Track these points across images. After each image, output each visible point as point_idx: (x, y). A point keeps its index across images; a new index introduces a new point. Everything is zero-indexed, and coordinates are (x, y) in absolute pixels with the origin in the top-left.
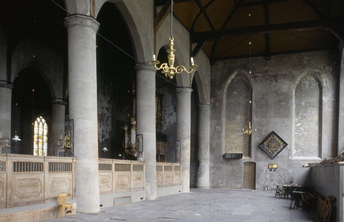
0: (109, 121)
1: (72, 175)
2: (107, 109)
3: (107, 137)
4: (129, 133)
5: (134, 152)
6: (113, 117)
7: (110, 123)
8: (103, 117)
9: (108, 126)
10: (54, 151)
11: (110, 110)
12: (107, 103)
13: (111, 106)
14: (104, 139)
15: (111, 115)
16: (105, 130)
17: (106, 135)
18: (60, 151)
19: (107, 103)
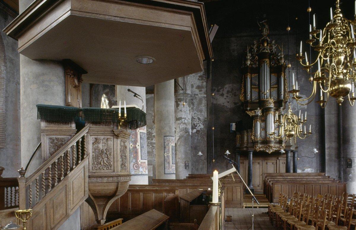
0: (203, 105)
1: (331, 189)
2: (198, 87)
3: (200, 127)
4: (264, 120)
5: (272, 147)
6: (208, 99)
7: (204, 108)
8: (192, 100)
9: (201, 111)
10: (164, 145)
11: (204, 90)
12: (198, 79)
13: (205, 84)
14: (195, 131)
15: (205, 96)
16: (196, 118)
17: (198, 125)
18: (172, 145)
19: (198, 79)
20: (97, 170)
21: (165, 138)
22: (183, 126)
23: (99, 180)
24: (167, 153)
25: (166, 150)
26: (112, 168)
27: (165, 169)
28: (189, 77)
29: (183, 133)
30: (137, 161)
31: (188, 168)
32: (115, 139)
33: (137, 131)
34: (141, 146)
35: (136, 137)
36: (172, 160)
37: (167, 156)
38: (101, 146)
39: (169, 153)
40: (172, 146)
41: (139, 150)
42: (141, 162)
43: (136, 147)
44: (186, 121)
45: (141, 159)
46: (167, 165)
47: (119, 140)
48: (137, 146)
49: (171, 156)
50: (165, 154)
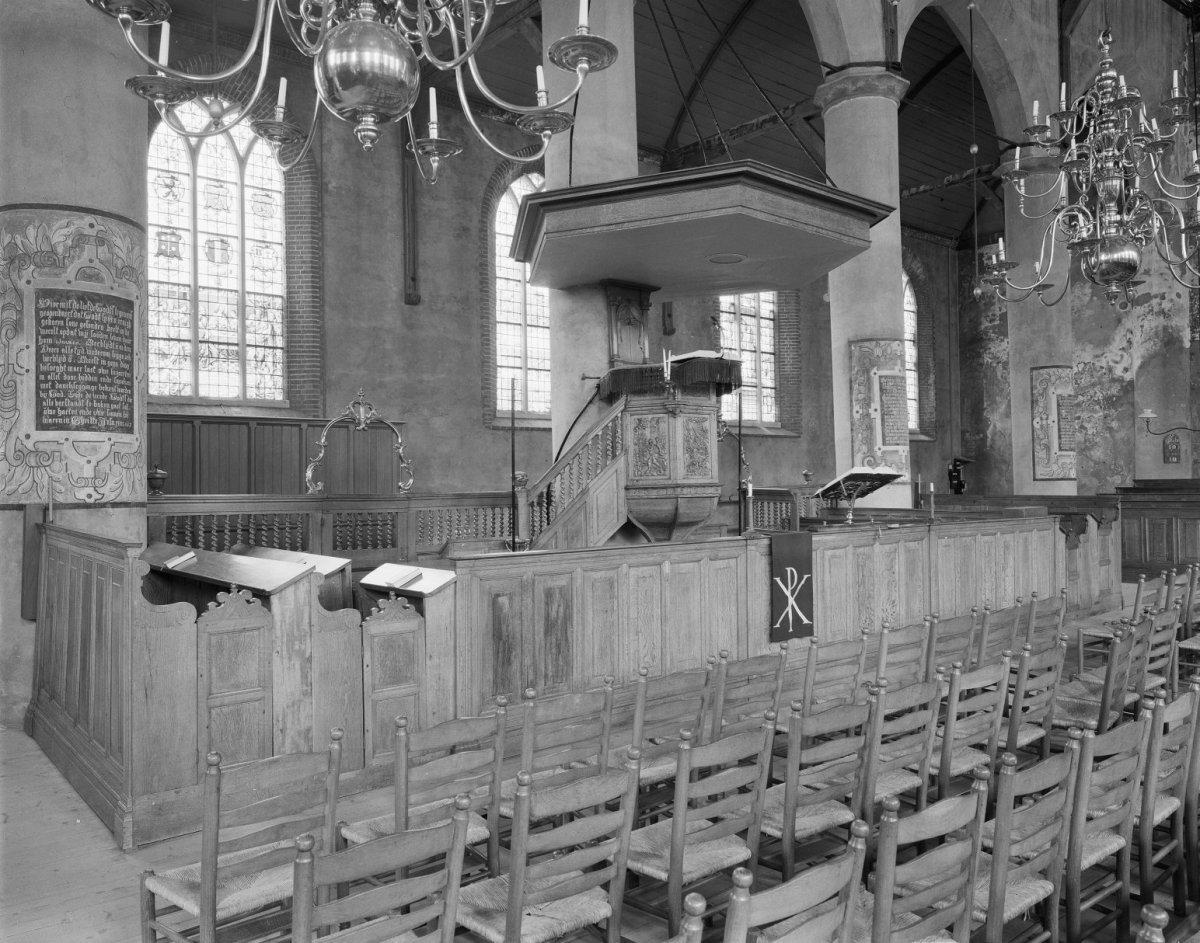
18: (1059, 392)
20: (641, 476)
21: (1035, 372)
22: (1153, 324)
23: (643, 493)
24: (1041, 419)
25: (1039, 409)
26: (667, 472)
27: (1034, 465)
28: (1172, 158)
29: (1155, 344)
30: (871, 449)
31: (1175, 459)
32: (671, 420)
33: (872, 373)
34: (882, 410)
35: (869, 389)
36: (1060, 437)
37: (1042, 426)
38: (647, 433)
39: (1047, 419)
40: (1060, 397)
41: (878, 422)
42: (884, 452)
43: (868, 415)
44: (1166, 305)
45: (884, 444)
46: (1041, 454)
47: (680, 421)
48: (871, 411)
49: (1056, 425)
50: (1035, 423)
